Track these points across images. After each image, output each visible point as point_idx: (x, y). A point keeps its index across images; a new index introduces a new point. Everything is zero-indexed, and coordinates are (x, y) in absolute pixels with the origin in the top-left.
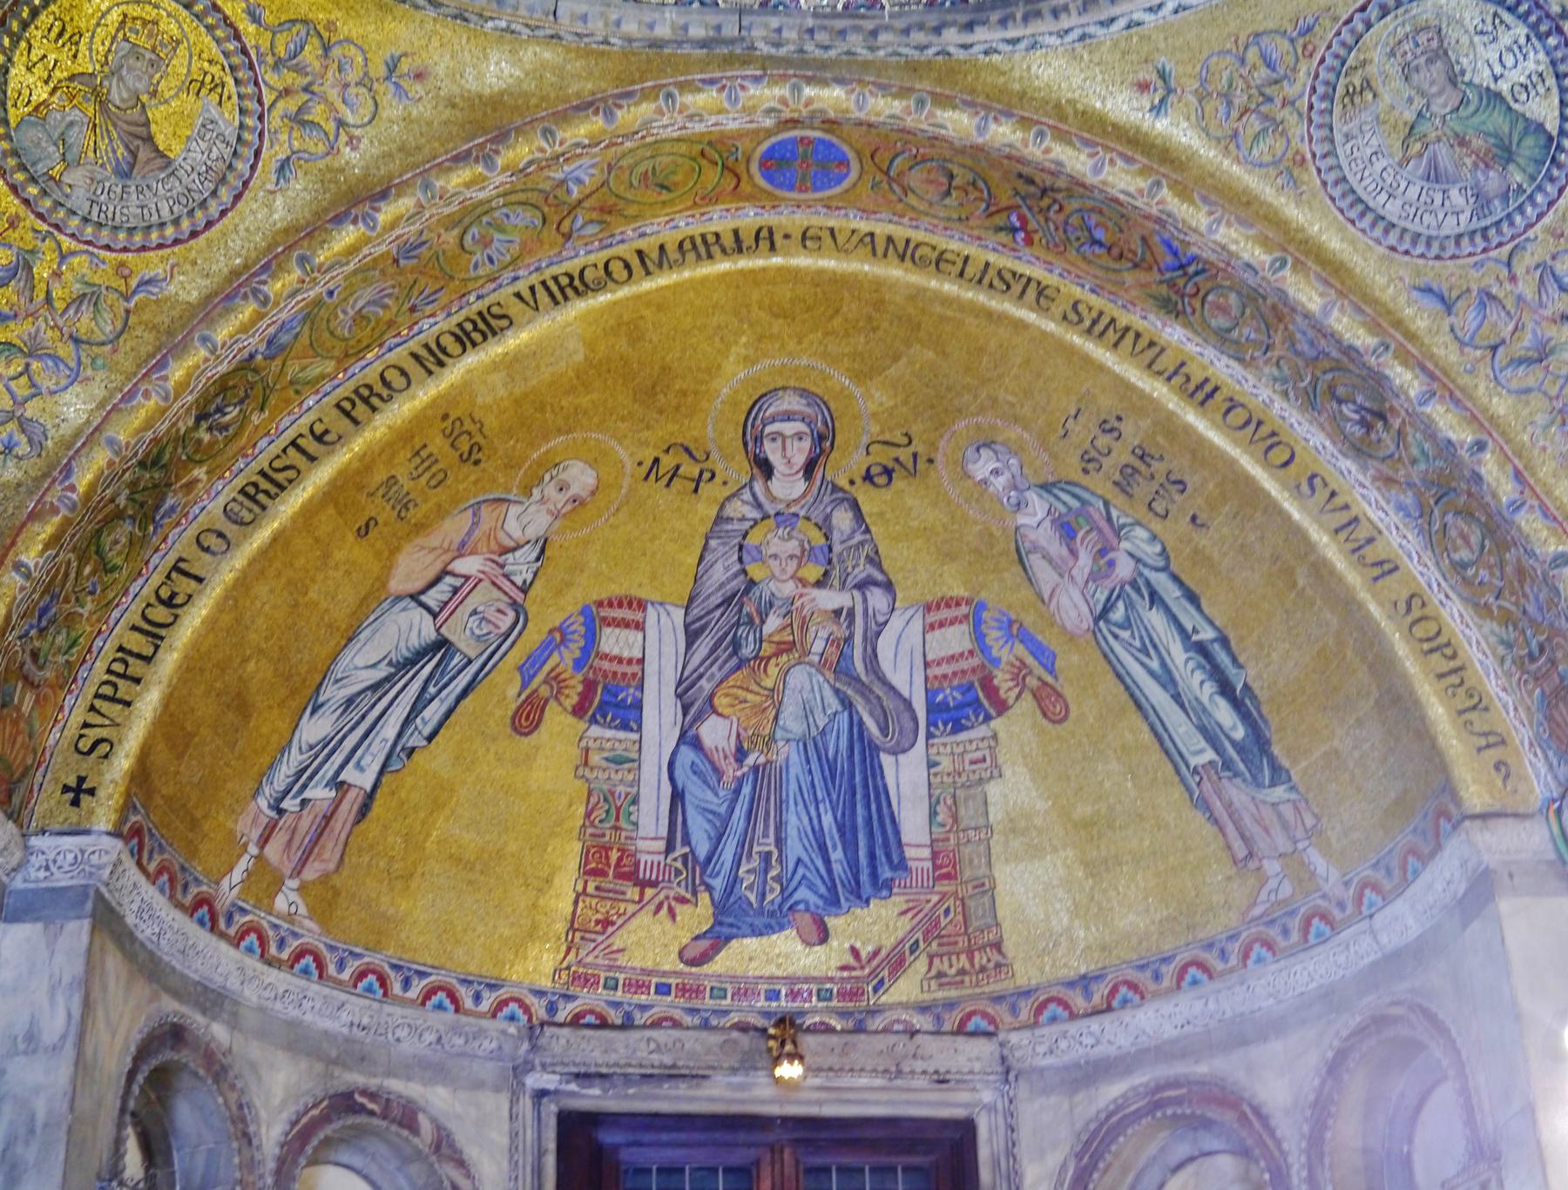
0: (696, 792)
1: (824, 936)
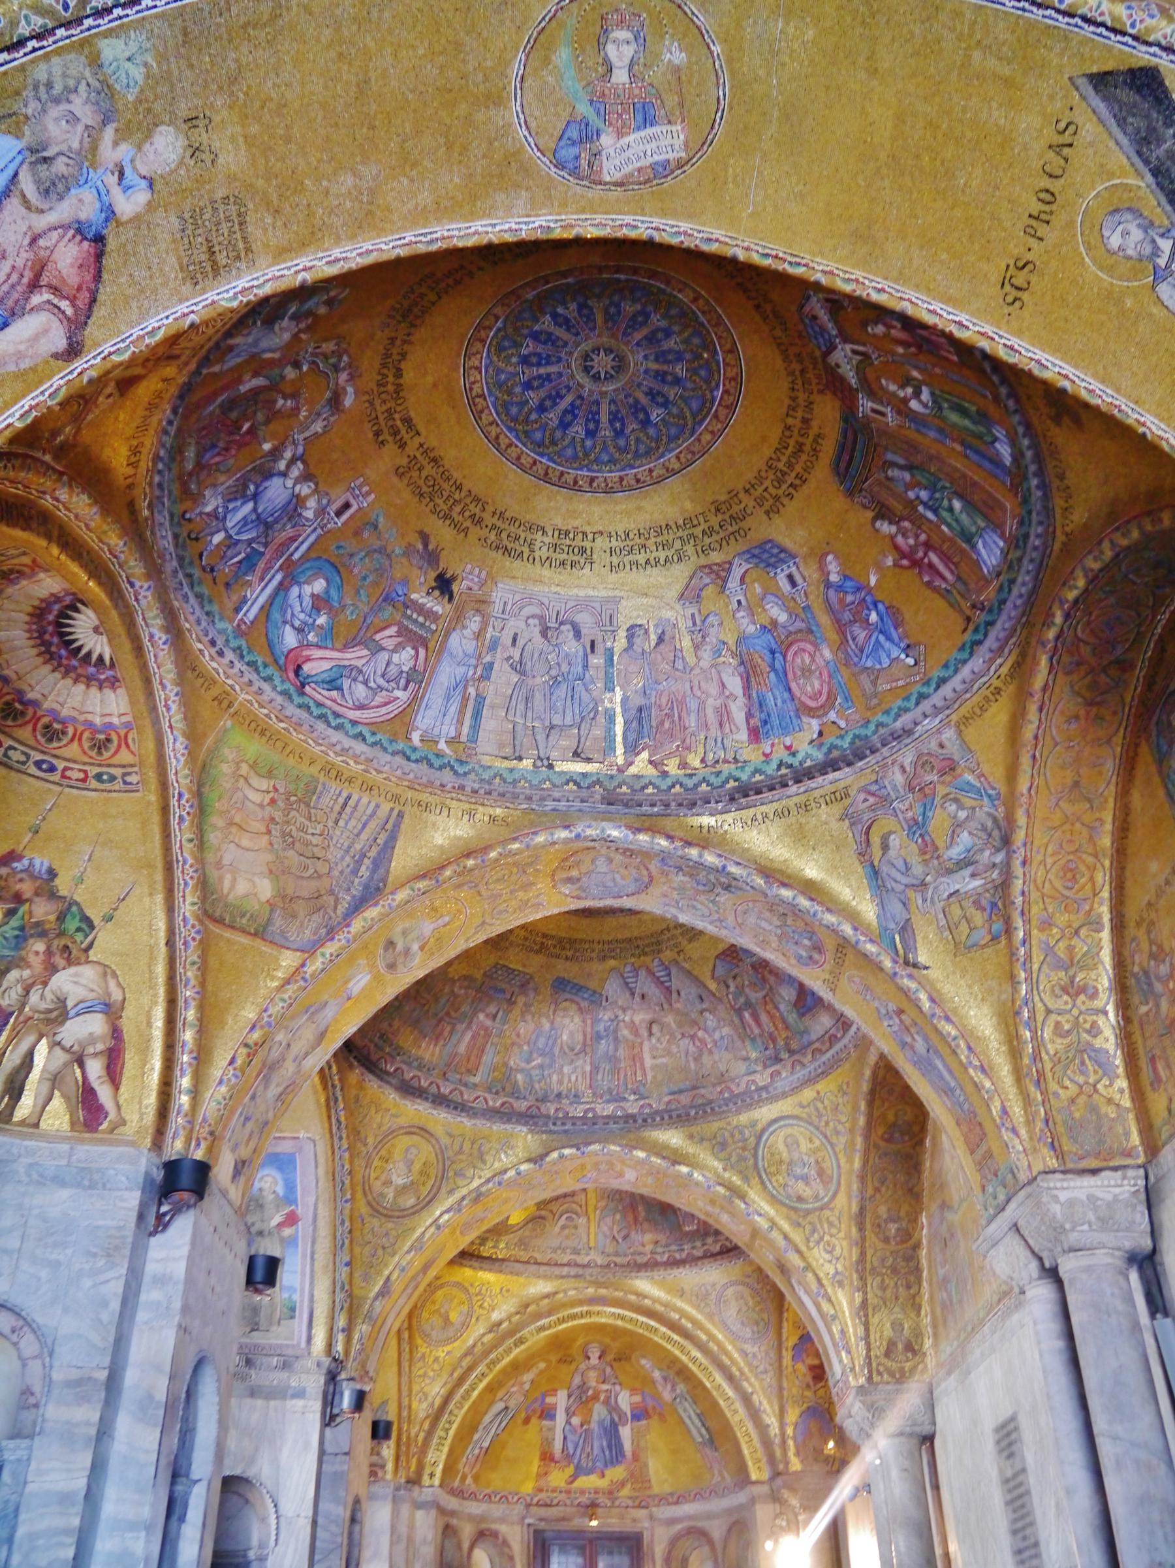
0: (570, 1437)
1: (603, 1476)
